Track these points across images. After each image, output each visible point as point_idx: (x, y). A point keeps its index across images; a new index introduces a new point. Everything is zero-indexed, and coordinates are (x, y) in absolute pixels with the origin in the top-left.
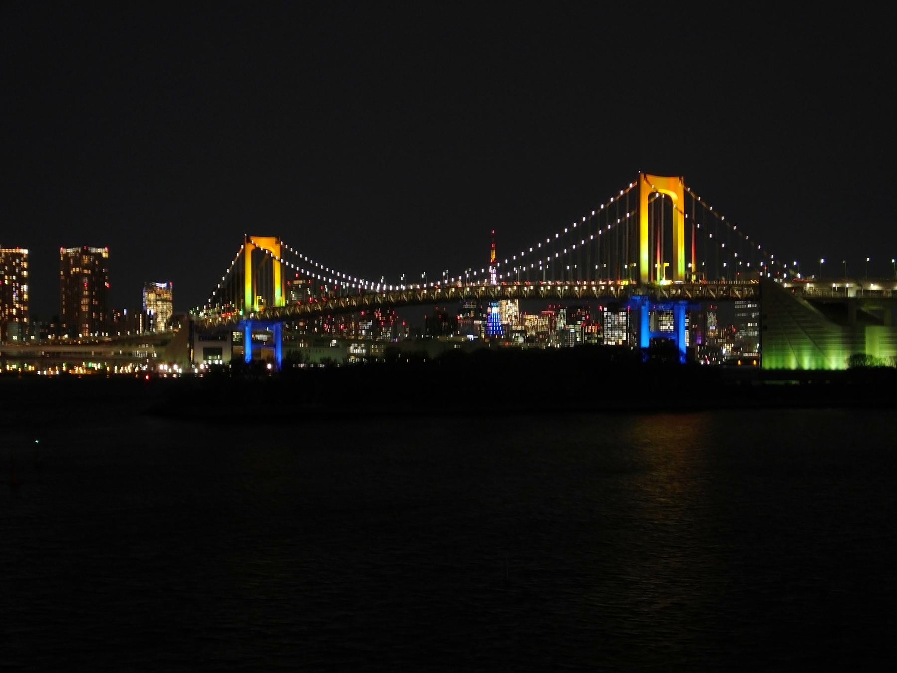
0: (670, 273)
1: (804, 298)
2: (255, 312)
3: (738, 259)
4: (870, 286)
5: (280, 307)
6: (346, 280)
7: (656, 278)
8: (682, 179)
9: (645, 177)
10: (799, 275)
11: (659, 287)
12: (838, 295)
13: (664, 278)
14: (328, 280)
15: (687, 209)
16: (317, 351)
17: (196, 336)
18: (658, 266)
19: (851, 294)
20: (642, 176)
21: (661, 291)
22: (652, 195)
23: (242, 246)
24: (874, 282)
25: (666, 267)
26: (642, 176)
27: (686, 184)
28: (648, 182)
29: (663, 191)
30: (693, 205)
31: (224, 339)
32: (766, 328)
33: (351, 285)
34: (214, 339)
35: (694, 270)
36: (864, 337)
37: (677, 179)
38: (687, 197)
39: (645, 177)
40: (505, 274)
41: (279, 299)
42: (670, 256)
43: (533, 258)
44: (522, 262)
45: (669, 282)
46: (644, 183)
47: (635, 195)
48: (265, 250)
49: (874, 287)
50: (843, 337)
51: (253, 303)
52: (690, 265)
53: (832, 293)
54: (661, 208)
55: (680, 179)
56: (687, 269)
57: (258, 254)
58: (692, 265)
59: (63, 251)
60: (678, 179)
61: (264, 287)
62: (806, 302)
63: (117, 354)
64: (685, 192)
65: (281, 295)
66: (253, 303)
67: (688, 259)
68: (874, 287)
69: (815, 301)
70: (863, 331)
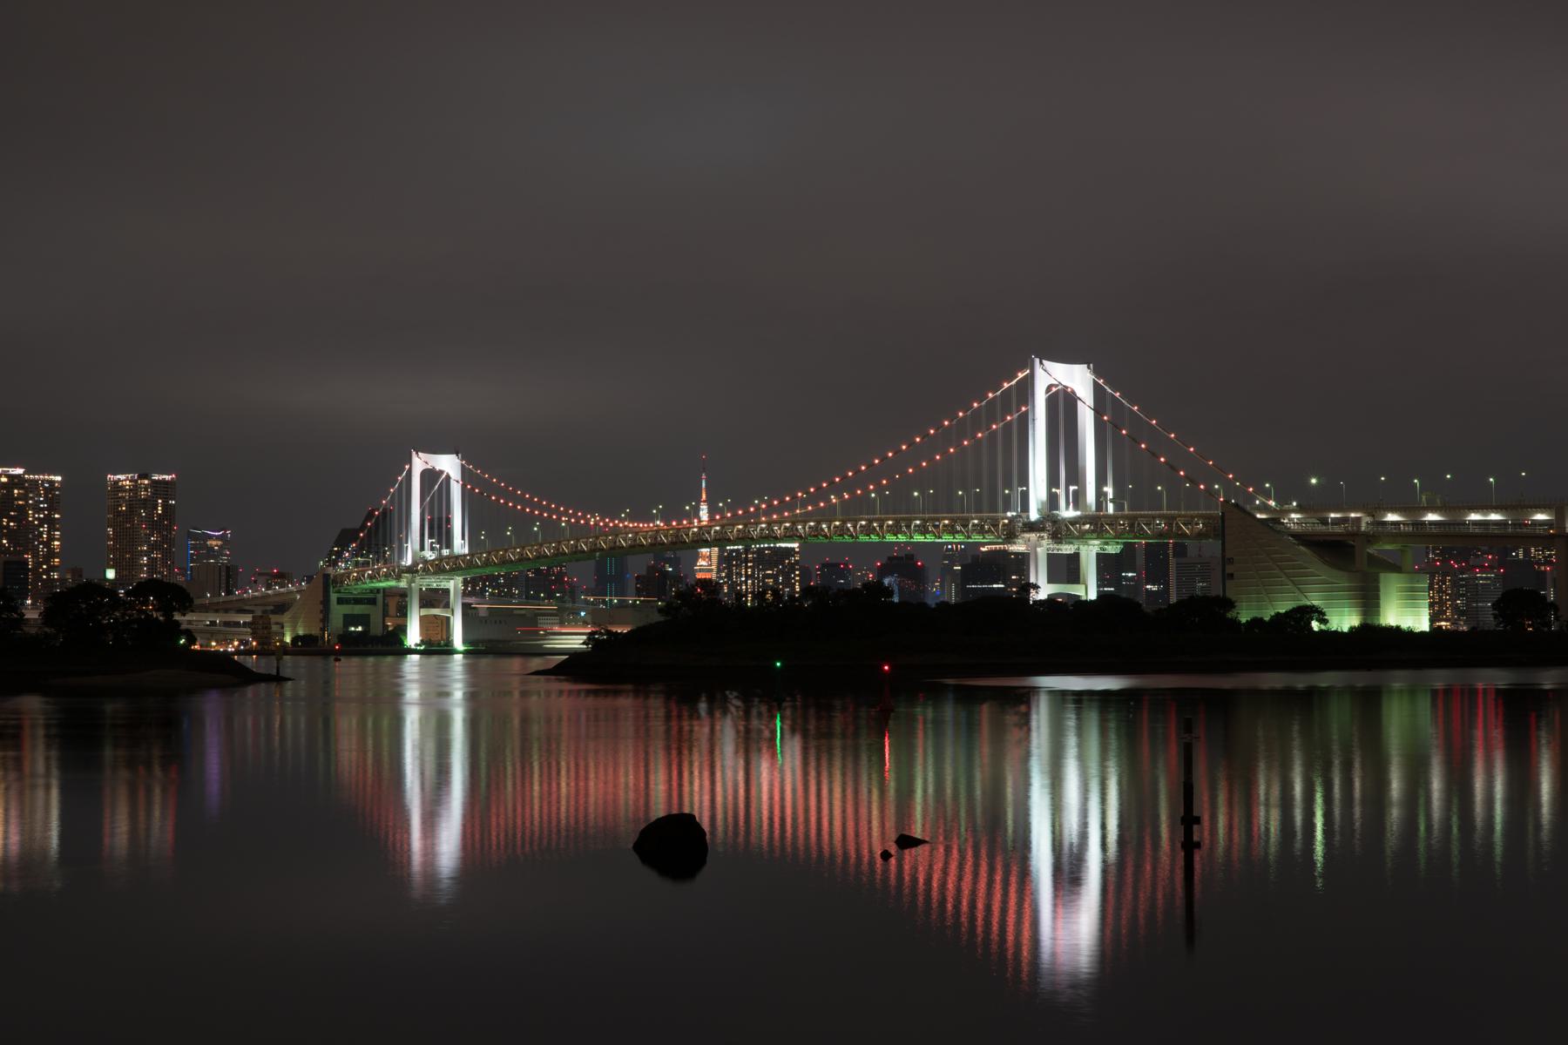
0: (1078, 499)
2: (425, 561)
3: (1186, 477)
4: (1385, 516)
5: (465, 556)
6: (565, 513)
7: (1057, 508)
8: (1091, 365)
10: (1272, 503)
11: (1064, 520)
12: (1338, 529)
14: (541, 514)
15: (1098, 411)
16: (496, 622)
17: (334, 597)
18: (1061, 492)
21: (1068, 527)
22: (1049, 388)
23: (407, 467)
24: (1393, 510)
25: (1074, 491)
26: (1037, 360)
27: (1097, 372)
28: (1045, 371)
29: (1064, 384)
30: (1109, 405)
31: (372, 602)
32: (1231, 576)
33: (569, 520)
34: (358, 601)
35: (1110, 496)
37: (1086, 365)
38: (1098, 391)
39: (1041, 363)
40: (816, 504)
41: (460, 546)
42: (1075, 476)
43: (860, 479)
44: (848, 485)
45: (1078, 513)
46: (1039, 371)
47: (1026, 388)
48: (441, 472)
49: (1392, 517)
50: (1349, 589)
51: (422, 548)
52: (1105, 489)
53: (1330, 529)
54: (1062, 403)
55: (1089, 368)
56: (1100, 494)
57: (430, 476)
58: (1109, 490)
59: (109, 476)
60: (1086, 365)
61: (438, 528)
63: (213, 623)
64: (1096, 384)
65: (463, 538)
66: (422, 548)
67: (1101, 481)
68: (1392, 517)
69: (1302, 538)
70: (1377, 581)
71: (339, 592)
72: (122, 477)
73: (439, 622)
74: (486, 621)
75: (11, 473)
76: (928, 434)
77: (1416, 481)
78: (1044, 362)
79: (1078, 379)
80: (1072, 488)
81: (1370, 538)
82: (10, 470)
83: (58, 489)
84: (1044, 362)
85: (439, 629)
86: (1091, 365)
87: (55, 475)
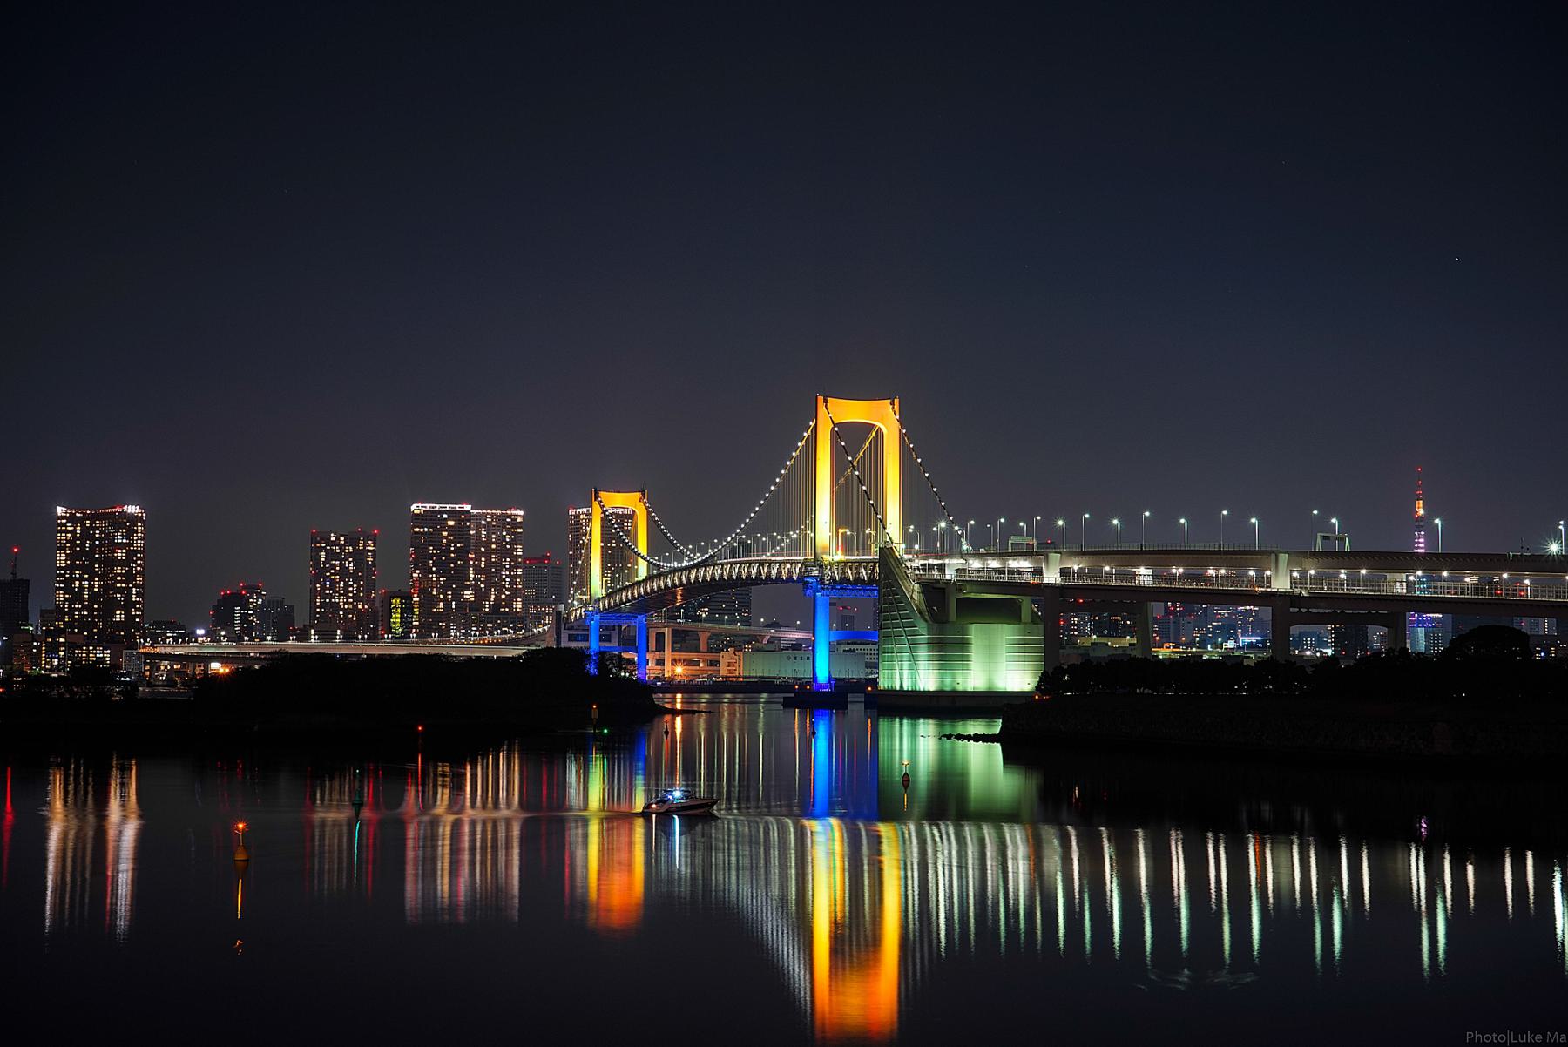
1: (918, 583)
8: (896, 401)
9: (826, 402)
13: (839, 552)
19: (950, 575)
20: (821, 399)
25: (842, 534)
26: (821, 399)
28: (827, 409)
36: (966, 641)
37: (889, 401)
39: (826, 402)
55: (892, 403)
59: (572, 511)
62: (917, 587)
70: (964, 631)
71: (571, 628)
72: (581, 510)
73: (737, 657)
74: (795, 658)
75: (458, 509)
76: (782, 474)
77: (1182, 521)
78: (829, 399)
79: (884, 417)
80: (841, 531)
81: (958, 586)
82: (457, 506)
83: (520, 525)
84: (829, 399)
85: (737, 665)
86: (896, 401)
87: (516, 509)
